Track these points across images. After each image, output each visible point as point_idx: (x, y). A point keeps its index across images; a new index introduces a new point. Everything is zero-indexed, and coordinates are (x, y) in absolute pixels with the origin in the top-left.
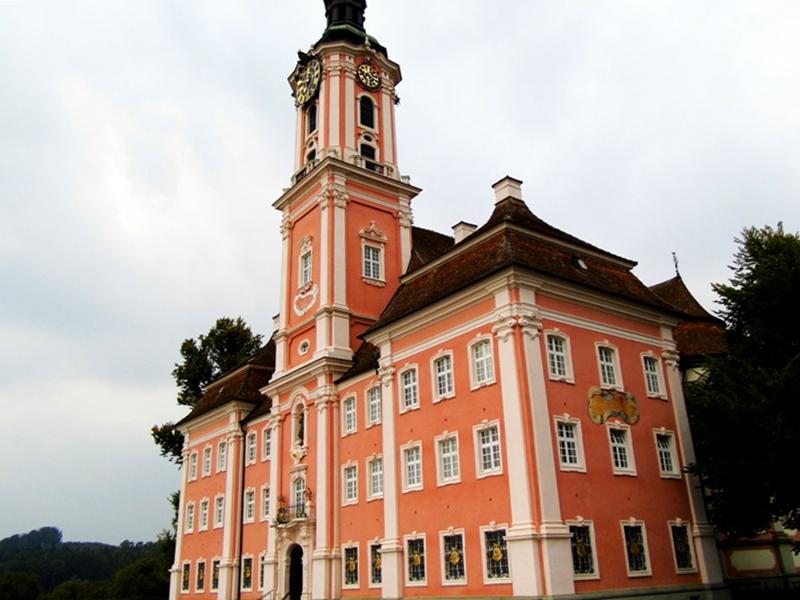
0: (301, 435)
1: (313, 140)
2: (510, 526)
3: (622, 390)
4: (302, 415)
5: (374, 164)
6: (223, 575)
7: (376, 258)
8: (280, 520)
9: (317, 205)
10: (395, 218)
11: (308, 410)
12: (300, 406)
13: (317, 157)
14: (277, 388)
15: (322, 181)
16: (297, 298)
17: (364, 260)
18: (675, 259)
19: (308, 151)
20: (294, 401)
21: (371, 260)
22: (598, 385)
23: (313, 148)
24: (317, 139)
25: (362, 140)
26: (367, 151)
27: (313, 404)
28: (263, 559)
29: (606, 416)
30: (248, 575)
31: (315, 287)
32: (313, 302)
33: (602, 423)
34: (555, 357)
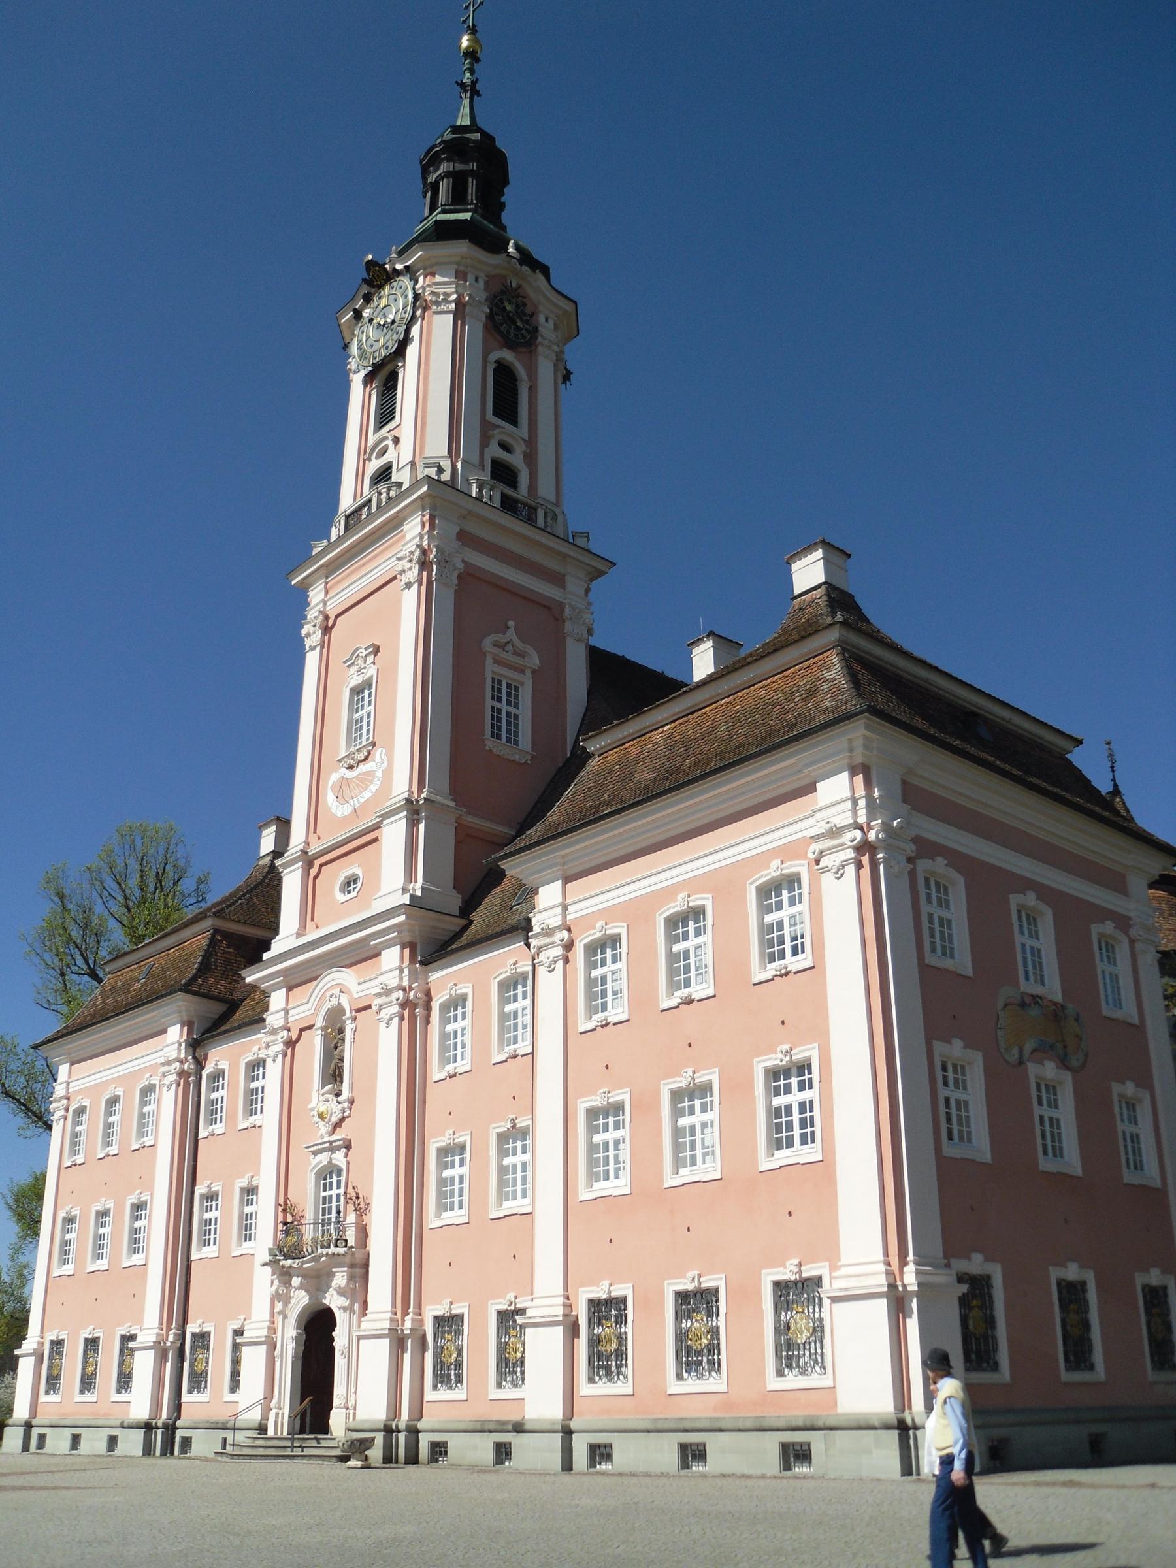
1: (389, 442)
2: (833, 1268)
3: (1059, 998)
5: (516, 501)
6: (143, 1365)
7: (513, 701)
9: (395, 578)
10: (557, 620)
11: (355, 1019)
13: (395, 477)
15: (405, 528)
16: (334, 777)
18: (1111, 755)
19: (374, 465)
22: (1017, 985)
24: (396, 441)
25: (494, 451)
26: (502, 473)
27: (369, 1007)
28: (238, 1333)
29: (1028, 1048)
31: (379, 754)
32: (374, 787)
33: (1021, 1063)
34: (936, 921)
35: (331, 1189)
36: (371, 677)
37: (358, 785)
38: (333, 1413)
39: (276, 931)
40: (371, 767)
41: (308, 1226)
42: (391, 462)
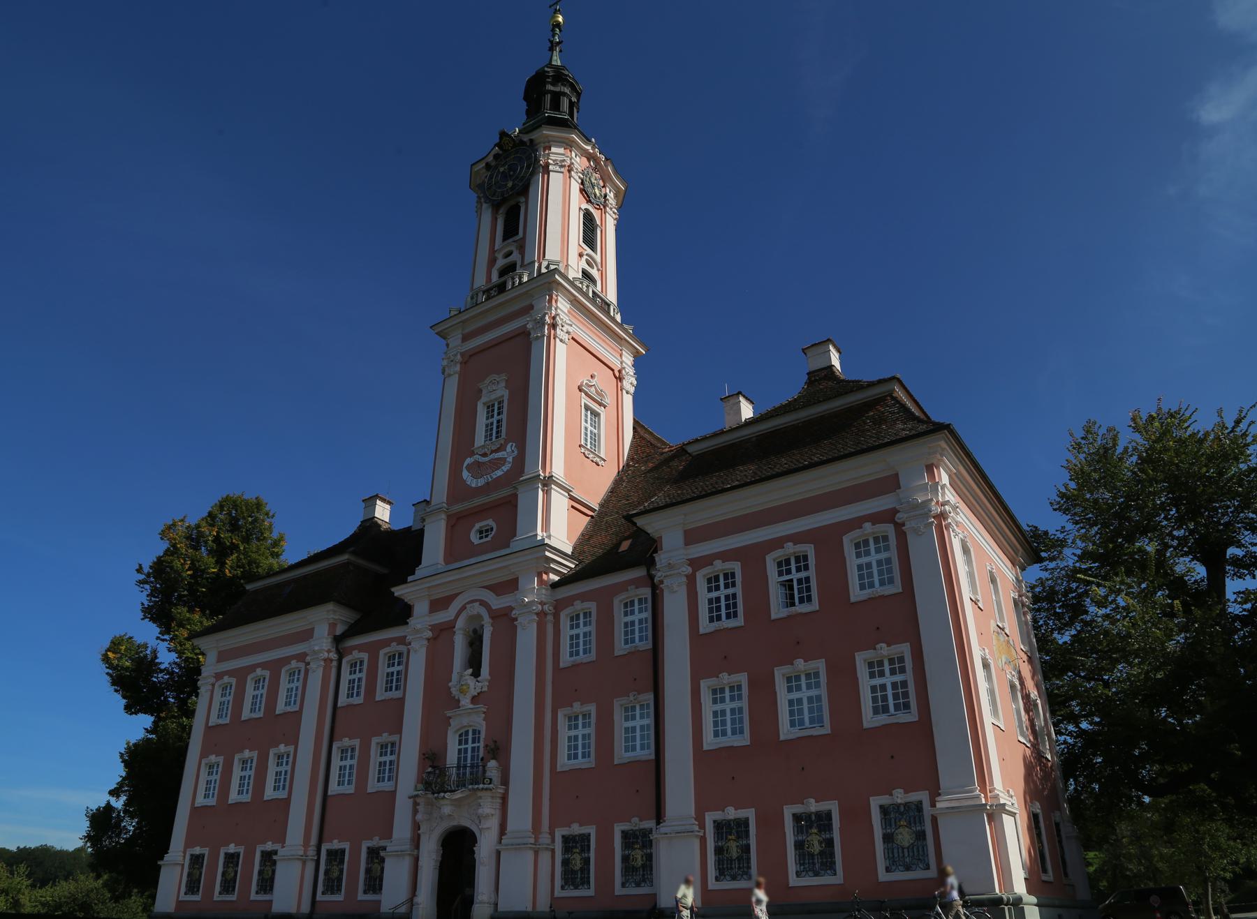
23: (511, 259)
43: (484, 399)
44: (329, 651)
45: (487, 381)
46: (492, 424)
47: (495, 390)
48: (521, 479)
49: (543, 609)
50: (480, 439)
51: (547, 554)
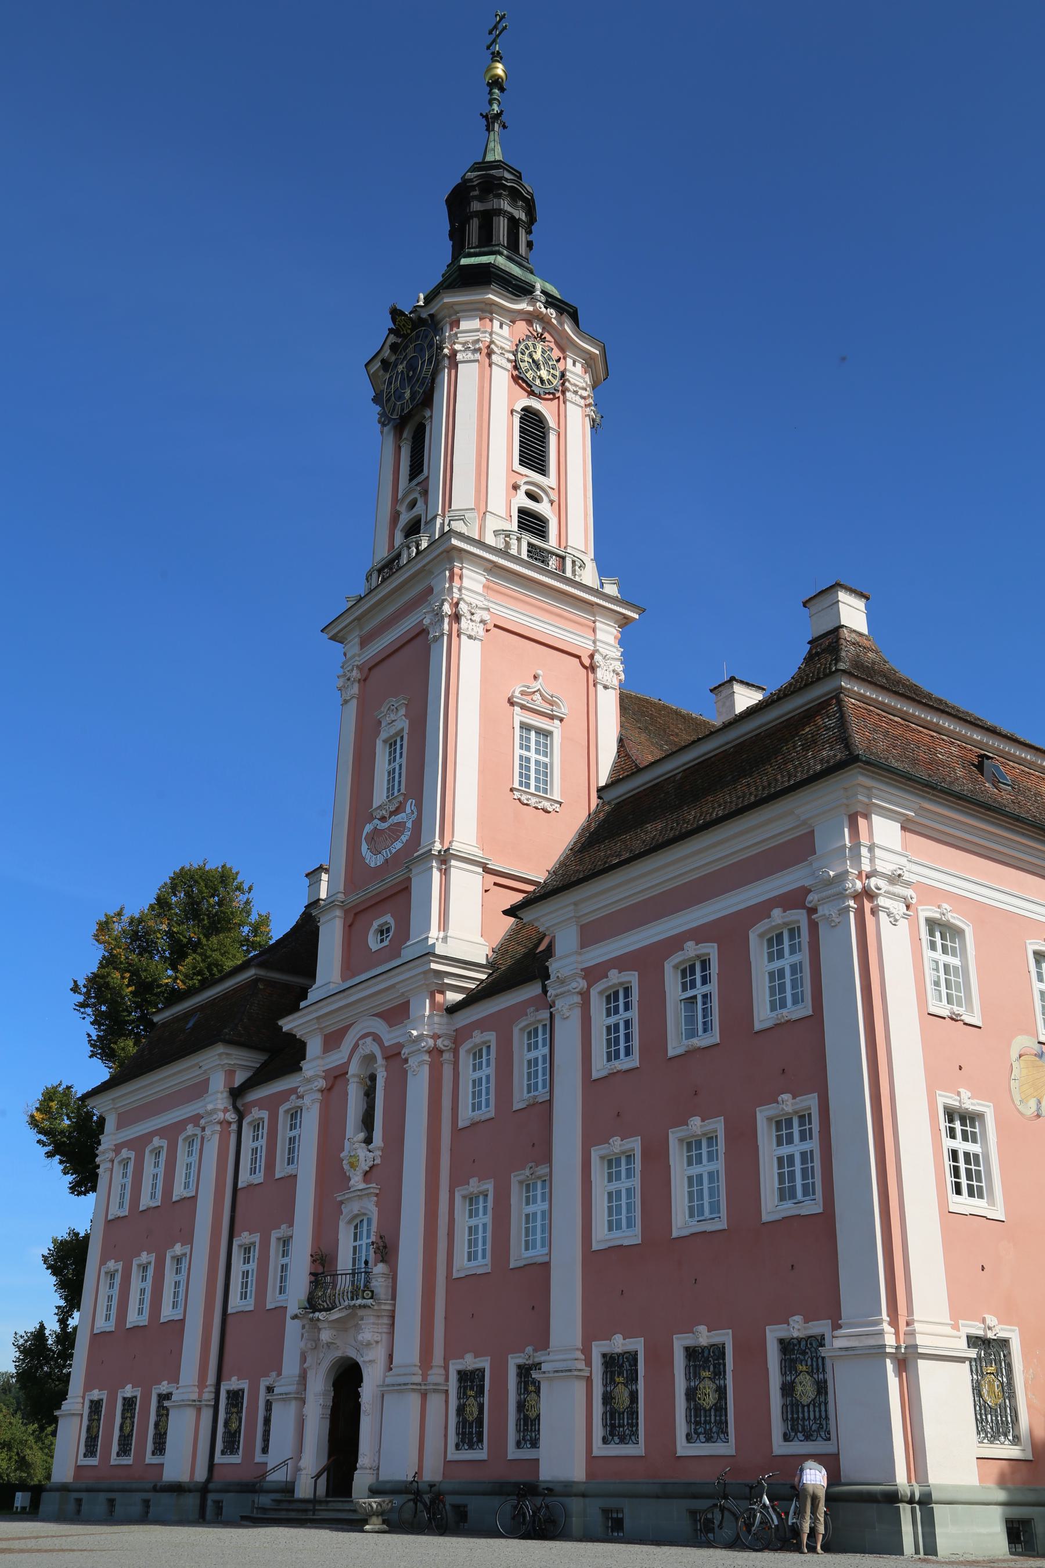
0: (368, 1122)
4: (373, 1078)
8: (312, 1304)
12: (370, 1058)
14: (318, 1018)
16: (368, 828)
17: (518, 752)
19: (405, 518)
20: (356, 1046)
21: (533, 755)
28: (270, 1389)
30: (234, 1426)
32: (404, 838)
35: (361, 1239)
36: (402, 730)
37: (390, 836)
38: (357, 1475)
39: (312, 975)
40: (403, 819)
41: (340, 1277)
42: (421, 515)
43: (384, 735)
44: (225, 1110)
45: (384, 709)
46: (394, 769)
47: (393, 721)
48: (416, 855)
49: (435, 1045)
50: (380, 795)
51: (434, 966)
